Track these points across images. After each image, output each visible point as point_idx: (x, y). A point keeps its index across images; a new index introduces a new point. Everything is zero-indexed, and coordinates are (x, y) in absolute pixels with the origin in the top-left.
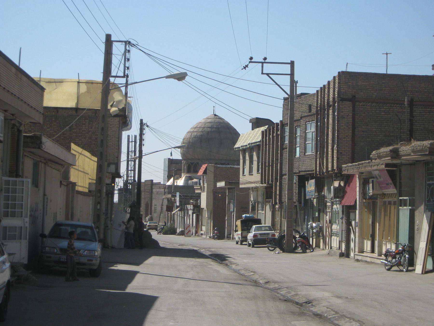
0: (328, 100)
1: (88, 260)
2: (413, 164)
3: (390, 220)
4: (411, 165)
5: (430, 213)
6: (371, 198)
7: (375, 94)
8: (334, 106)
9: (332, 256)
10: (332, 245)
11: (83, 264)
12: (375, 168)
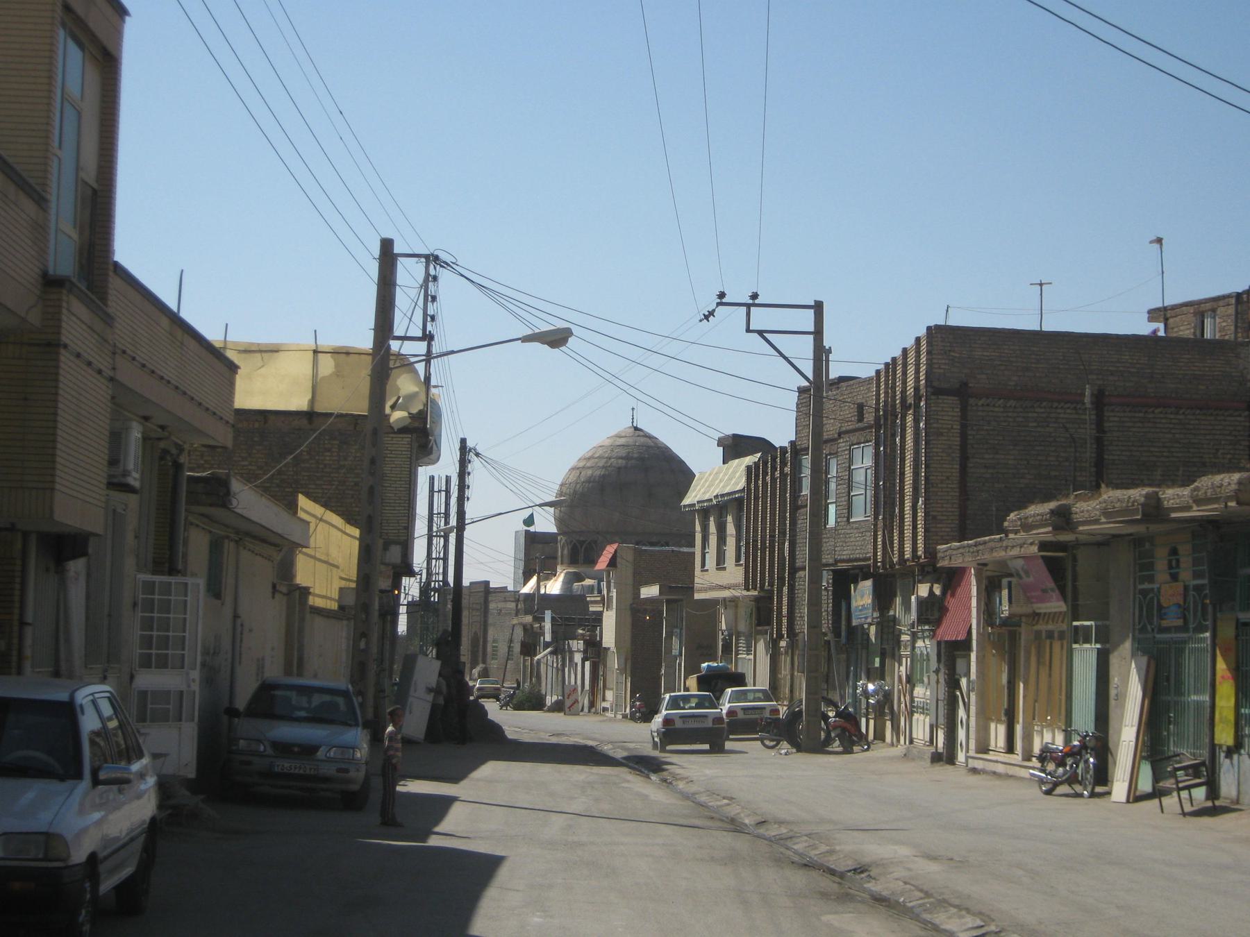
0: (904, 391)
1: (339, 770)
2: (1106, 543)
3: (1050, 675)
4: (1099, 544)
5: (1144, 659)
6: (1006, 622)
7: (1015, 378)
8: (917, 406)
9: (913, 759)
10: (914, 736)
11: (326, 779)
12: (1015, 552)
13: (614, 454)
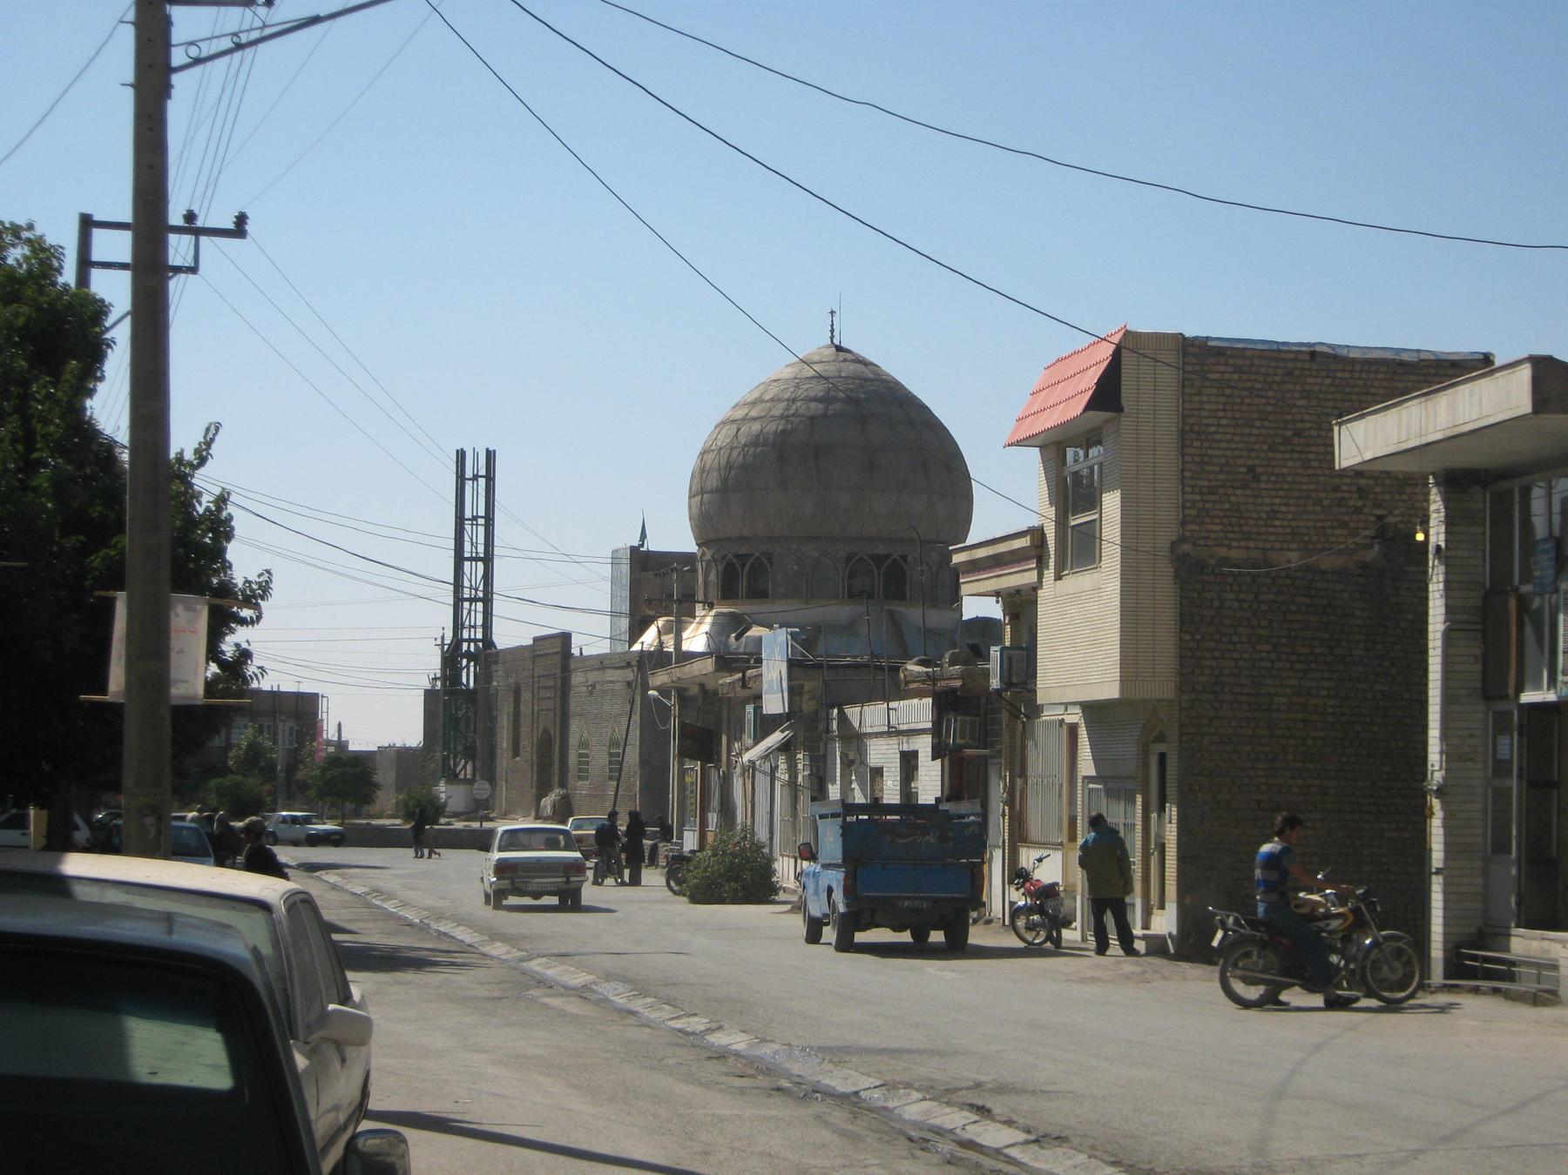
13: (801, 393)
